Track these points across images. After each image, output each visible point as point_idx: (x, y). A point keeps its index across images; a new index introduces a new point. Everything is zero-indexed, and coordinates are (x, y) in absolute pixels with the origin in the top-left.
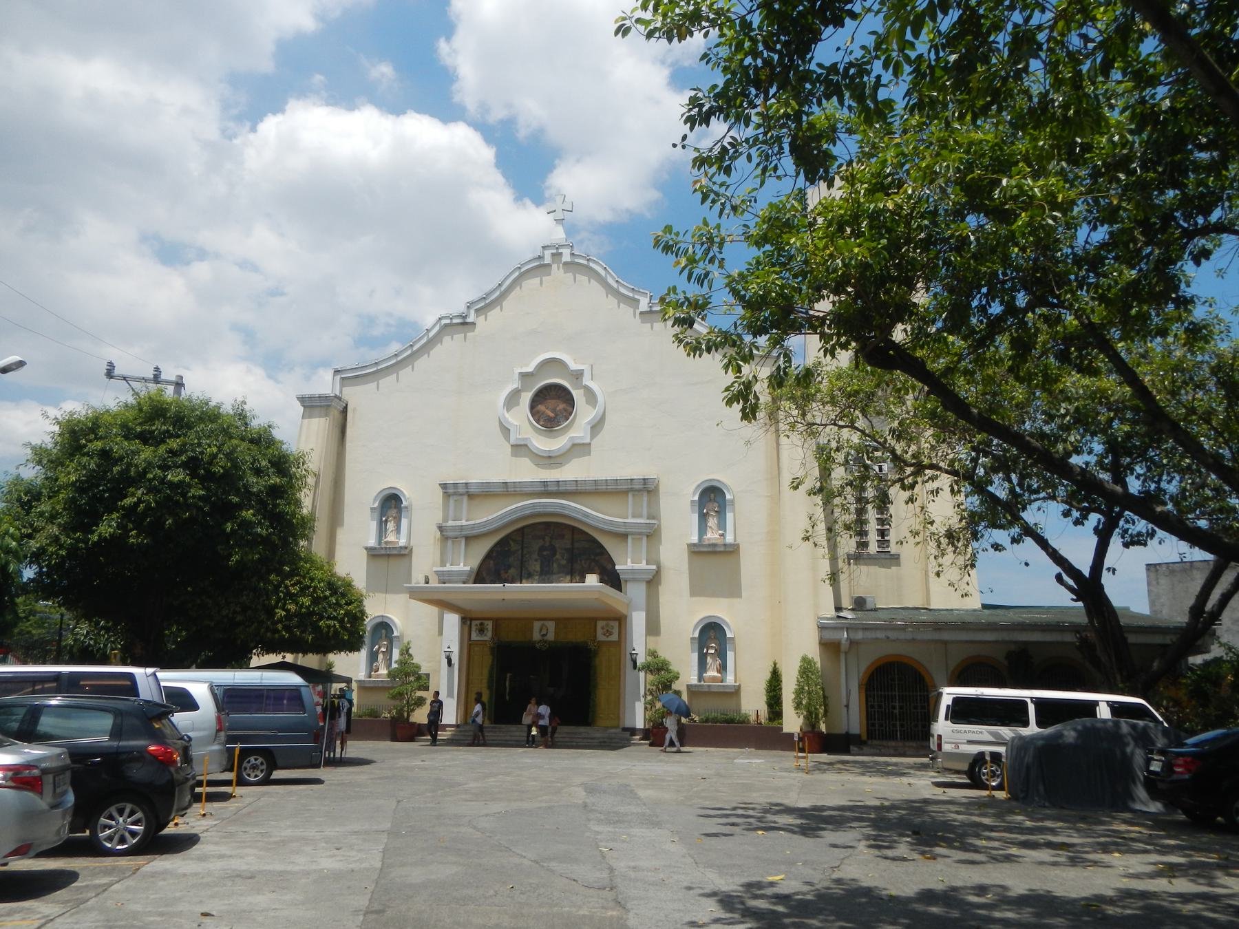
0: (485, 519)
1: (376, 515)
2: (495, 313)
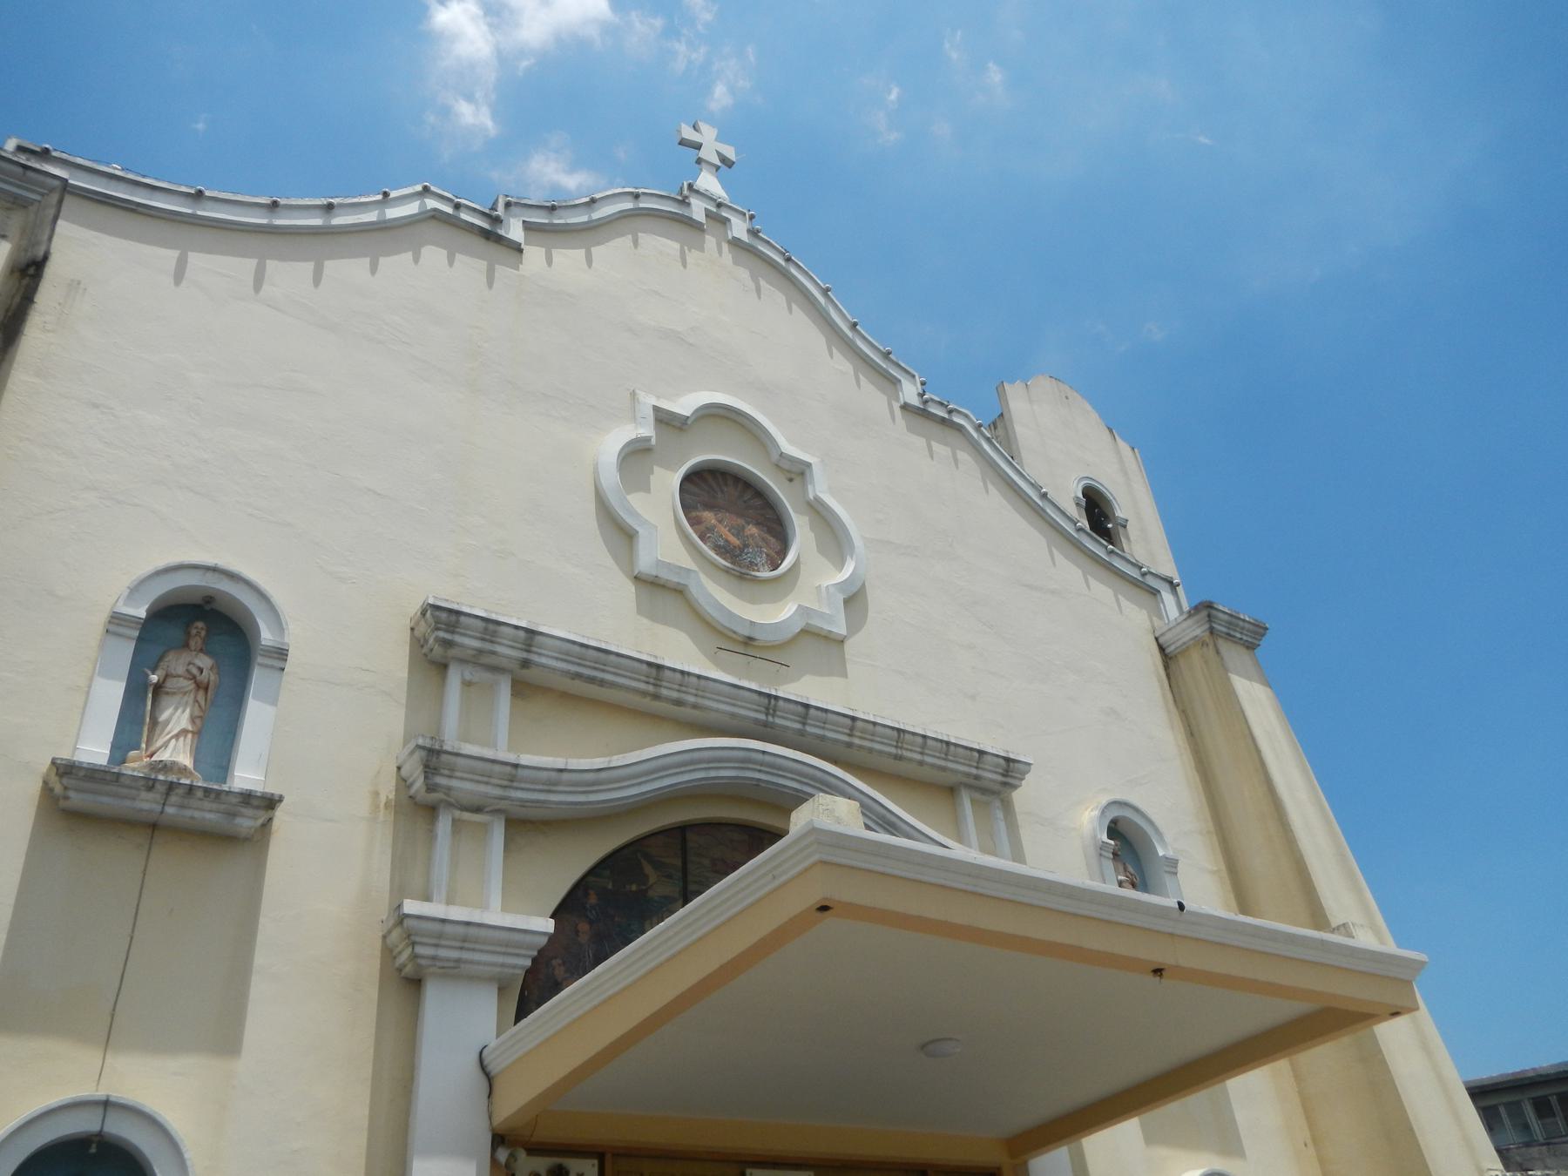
0: (599, 762)
1: (125, 652)
2: (568, 259)
